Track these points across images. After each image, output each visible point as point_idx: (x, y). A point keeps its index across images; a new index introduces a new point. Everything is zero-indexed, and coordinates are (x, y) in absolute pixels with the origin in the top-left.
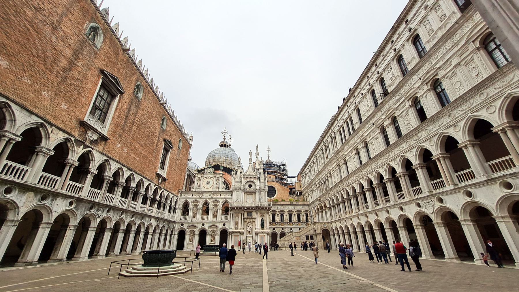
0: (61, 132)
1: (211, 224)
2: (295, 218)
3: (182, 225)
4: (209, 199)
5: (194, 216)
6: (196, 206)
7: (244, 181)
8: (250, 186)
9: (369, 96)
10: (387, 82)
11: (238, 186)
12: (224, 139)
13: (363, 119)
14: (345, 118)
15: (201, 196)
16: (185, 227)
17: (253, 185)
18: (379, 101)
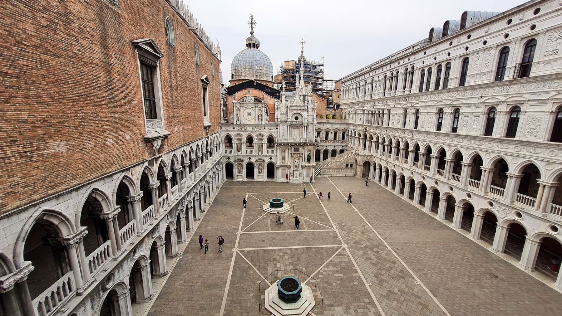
0: (137, 167)
1: (257, 158)
2: (331, 136)
3: (229, 158)
4: (252, 132)
5: (239, 150)
6: (240, 140)
7: (290, 113)
8: (297, 118)
9: (495, 54)
10: (538, 54)
11: (284, 118)
12: (252, 34)
13: (469, 82)
14: (438, 60)
15: (243, 129)
16: (232, 160)
17: (300, 117)
18: (509, 75)
